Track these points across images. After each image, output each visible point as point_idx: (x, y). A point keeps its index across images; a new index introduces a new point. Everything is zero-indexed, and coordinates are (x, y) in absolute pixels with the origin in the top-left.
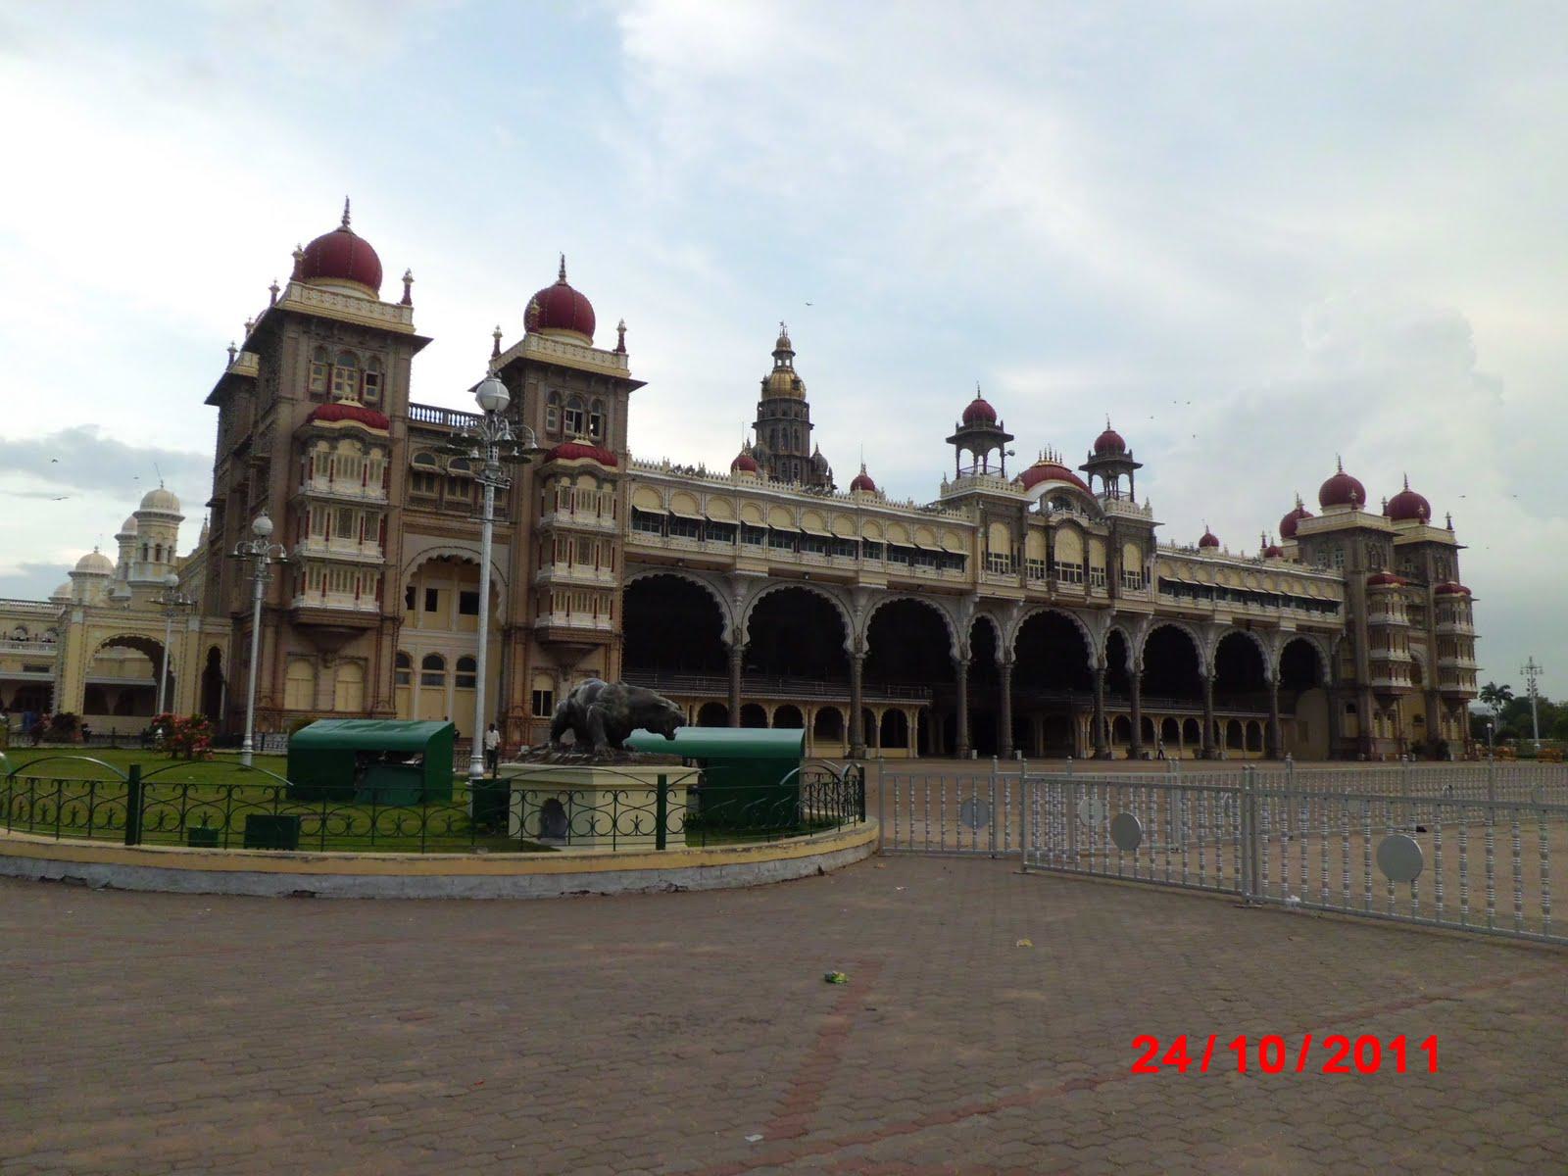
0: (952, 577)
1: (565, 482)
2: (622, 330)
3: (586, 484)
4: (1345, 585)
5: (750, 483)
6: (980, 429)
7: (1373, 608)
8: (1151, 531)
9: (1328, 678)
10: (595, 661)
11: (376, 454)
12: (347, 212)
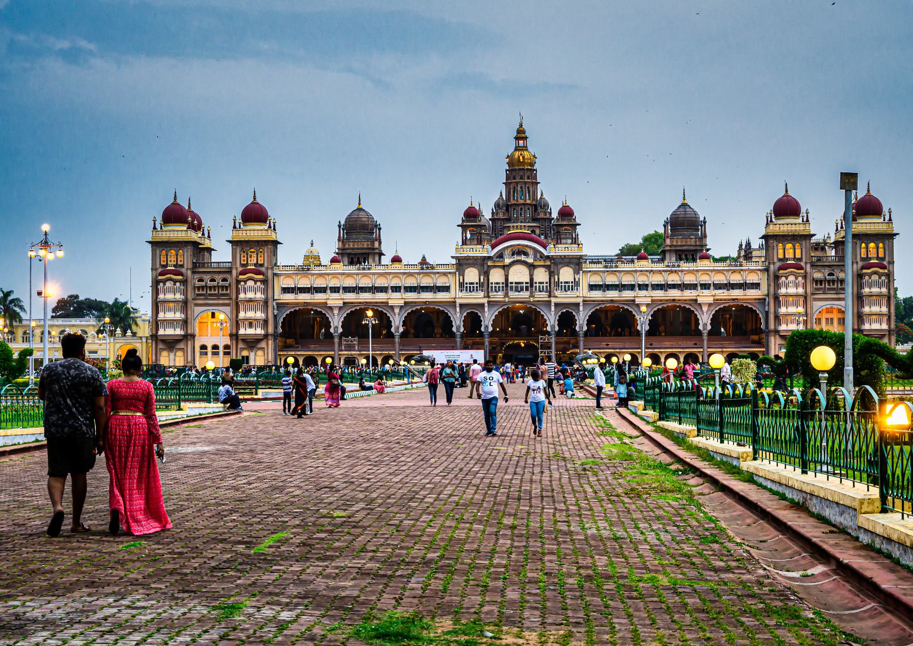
0: (442, 296)
1: (242, 283)
3: (250, 283)
4: (767, 270)
5: (339, 268)
9: (763, 326)
10: (263, 344)
11: (178, 284)
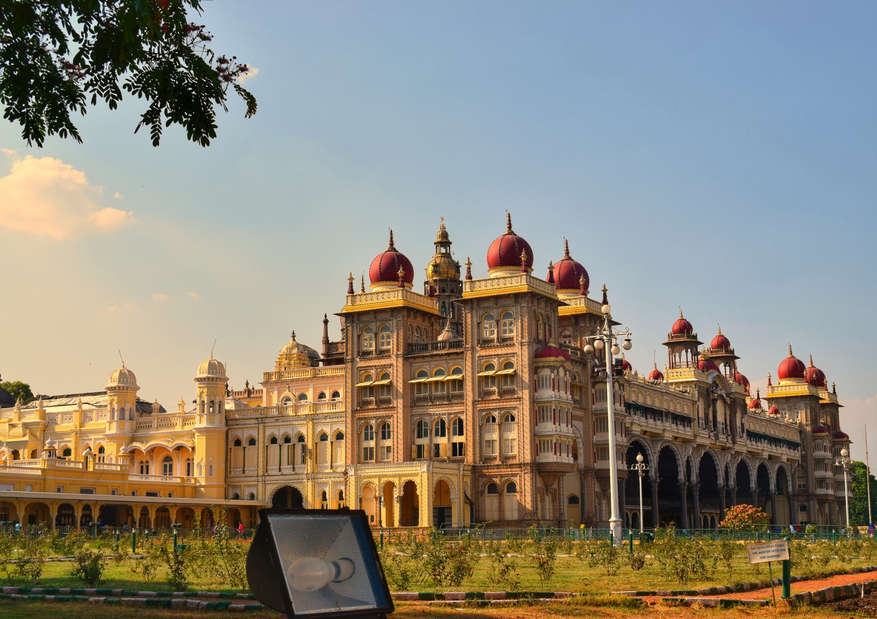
2: (605, 291)
4: (800, 432)
6: (683, 337)
7: (817, 448)
8: (744, 400)
9: (790, 489)
12: (510, 221)
